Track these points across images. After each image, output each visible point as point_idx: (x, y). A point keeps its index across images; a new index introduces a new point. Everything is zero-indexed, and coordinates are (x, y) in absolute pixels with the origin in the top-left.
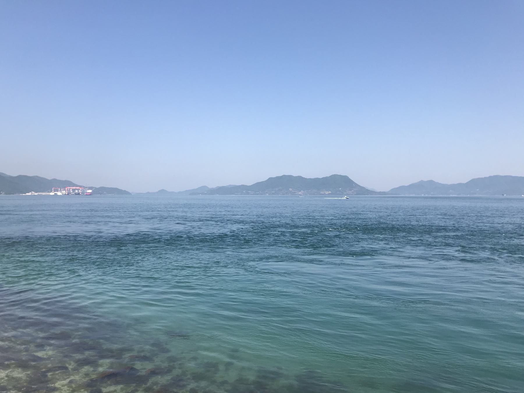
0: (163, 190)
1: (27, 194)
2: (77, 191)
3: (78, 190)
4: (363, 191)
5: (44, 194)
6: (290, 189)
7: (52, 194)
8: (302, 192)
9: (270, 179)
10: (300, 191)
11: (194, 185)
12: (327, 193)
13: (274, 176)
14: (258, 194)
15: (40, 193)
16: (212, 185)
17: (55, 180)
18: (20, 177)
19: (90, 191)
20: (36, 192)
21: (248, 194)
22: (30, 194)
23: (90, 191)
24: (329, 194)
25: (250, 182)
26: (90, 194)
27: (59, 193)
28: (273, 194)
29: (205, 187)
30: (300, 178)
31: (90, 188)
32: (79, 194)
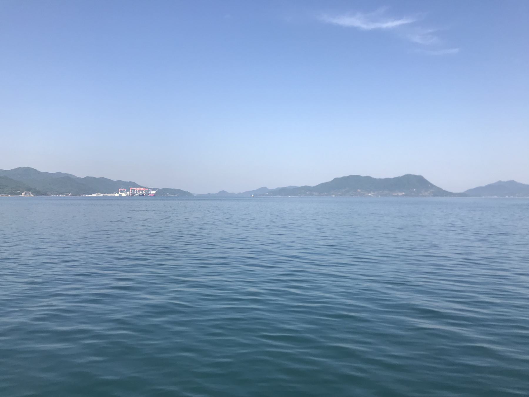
0: (223, 191)
1: (93, 195)
2: (141, 192)
3: (142, 191)
4: (439, 192)
5: (109, 195)
6: (359, 190)
7: (117, 195)
8: (372, 193)
9: (336, 180)
10: (369, 192)
11: (255, 187)
12: (400, 194)
13: (340, 176)
14: (323, 196)
15: (105, 195)
16: (273, 186)
17: (120, 181)
19: (154, 192)
21: (312, 195)
22: (95, 195)
23: (154, 192)
24: (403, 195)
25: (313, 183)
26: (154, 195)
27: (124, 195)
28: (341, 195)
29: (265, 188)
30: (368, 178)
31: (154, 189)
32: (143, 195)
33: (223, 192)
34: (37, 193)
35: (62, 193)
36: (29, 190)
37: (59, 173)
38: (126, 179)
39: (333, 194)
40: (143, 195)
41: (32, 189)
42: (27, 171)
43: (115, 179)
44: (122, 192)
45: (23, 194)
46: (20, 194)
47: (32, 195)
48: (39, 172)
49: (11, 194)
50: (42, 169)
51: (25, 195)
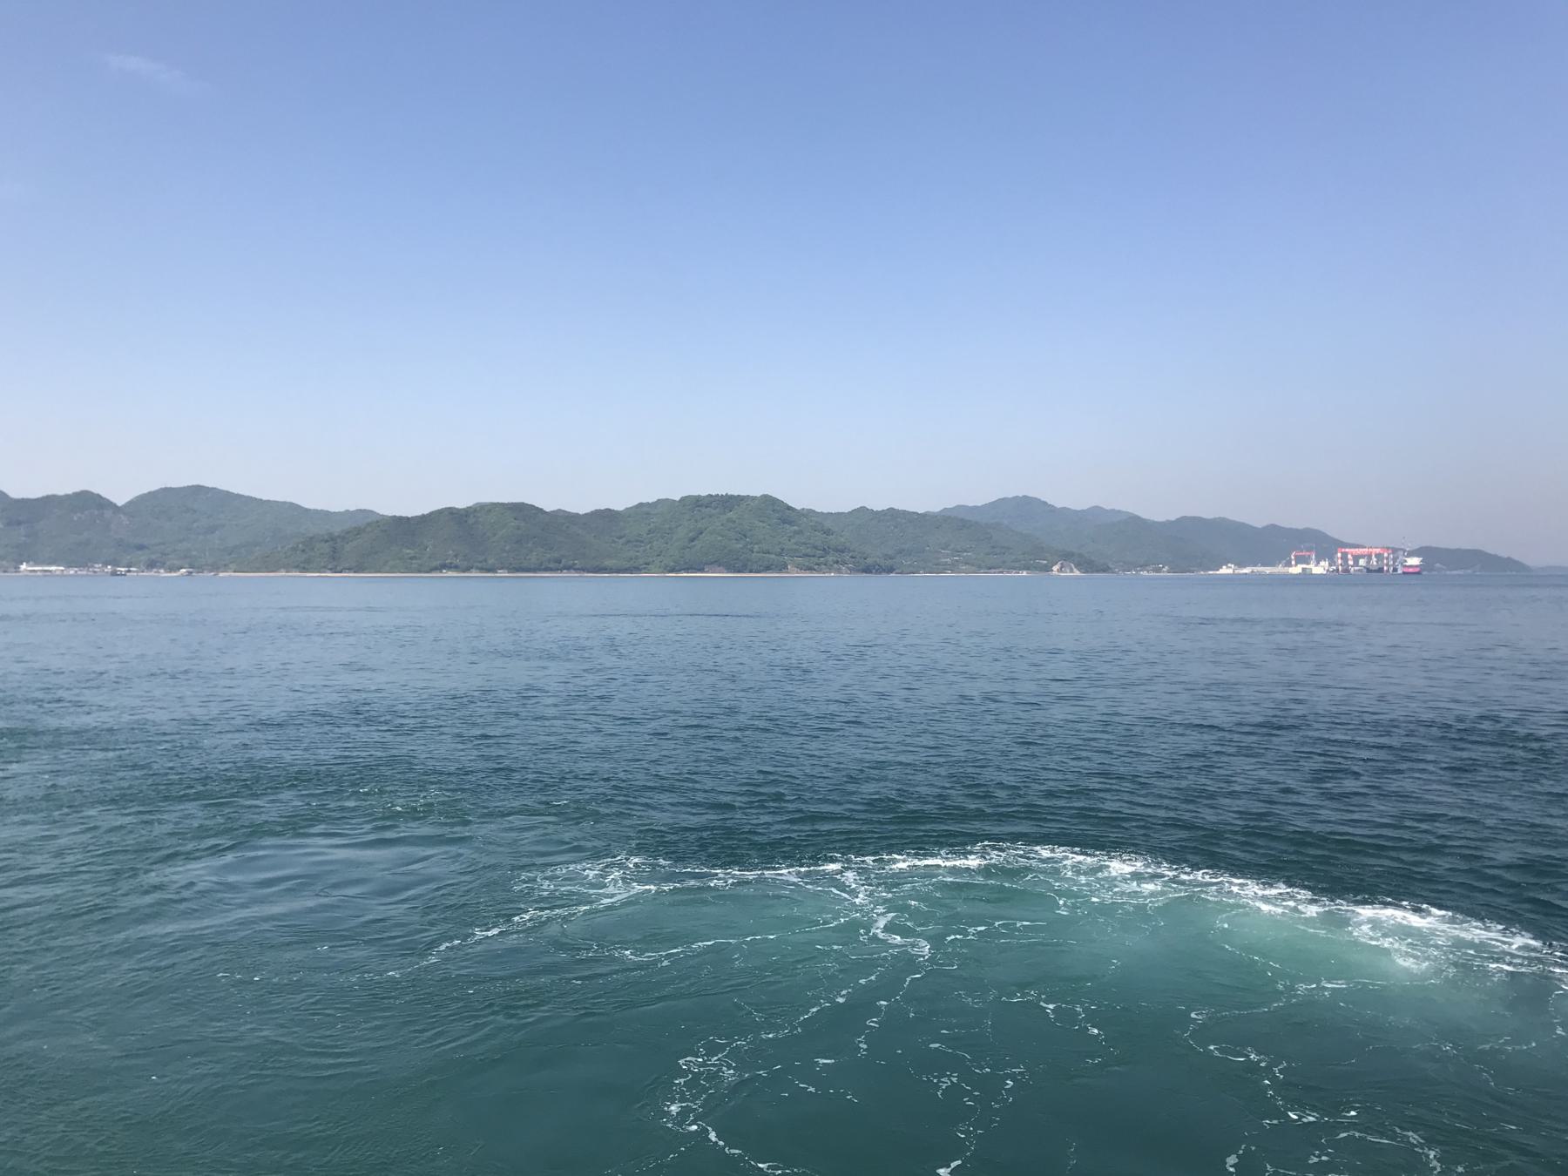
5: (1268, 570)
7: (1296, 570)
15: (1256, 569)
19: (1414, 561)
20: (1241, 565)
22: (1224, 570)
23: (1414, 561)
26: (1417, 572)
32: (1380, 570)
34: (1088, 565)
35: (1144, 566)
36: (1067, 557)
37: (1096, 510)
40: (1380, 570)
41: (1073, 554)
42: (1026, 506)
43: (1259, 521)
44: (1306, 560)
45: (1055, 568)
46: (1048, 569)
47: (1077, 573)
49: (1027, 568)
50: (1058, 501)
51: (1060, 570)
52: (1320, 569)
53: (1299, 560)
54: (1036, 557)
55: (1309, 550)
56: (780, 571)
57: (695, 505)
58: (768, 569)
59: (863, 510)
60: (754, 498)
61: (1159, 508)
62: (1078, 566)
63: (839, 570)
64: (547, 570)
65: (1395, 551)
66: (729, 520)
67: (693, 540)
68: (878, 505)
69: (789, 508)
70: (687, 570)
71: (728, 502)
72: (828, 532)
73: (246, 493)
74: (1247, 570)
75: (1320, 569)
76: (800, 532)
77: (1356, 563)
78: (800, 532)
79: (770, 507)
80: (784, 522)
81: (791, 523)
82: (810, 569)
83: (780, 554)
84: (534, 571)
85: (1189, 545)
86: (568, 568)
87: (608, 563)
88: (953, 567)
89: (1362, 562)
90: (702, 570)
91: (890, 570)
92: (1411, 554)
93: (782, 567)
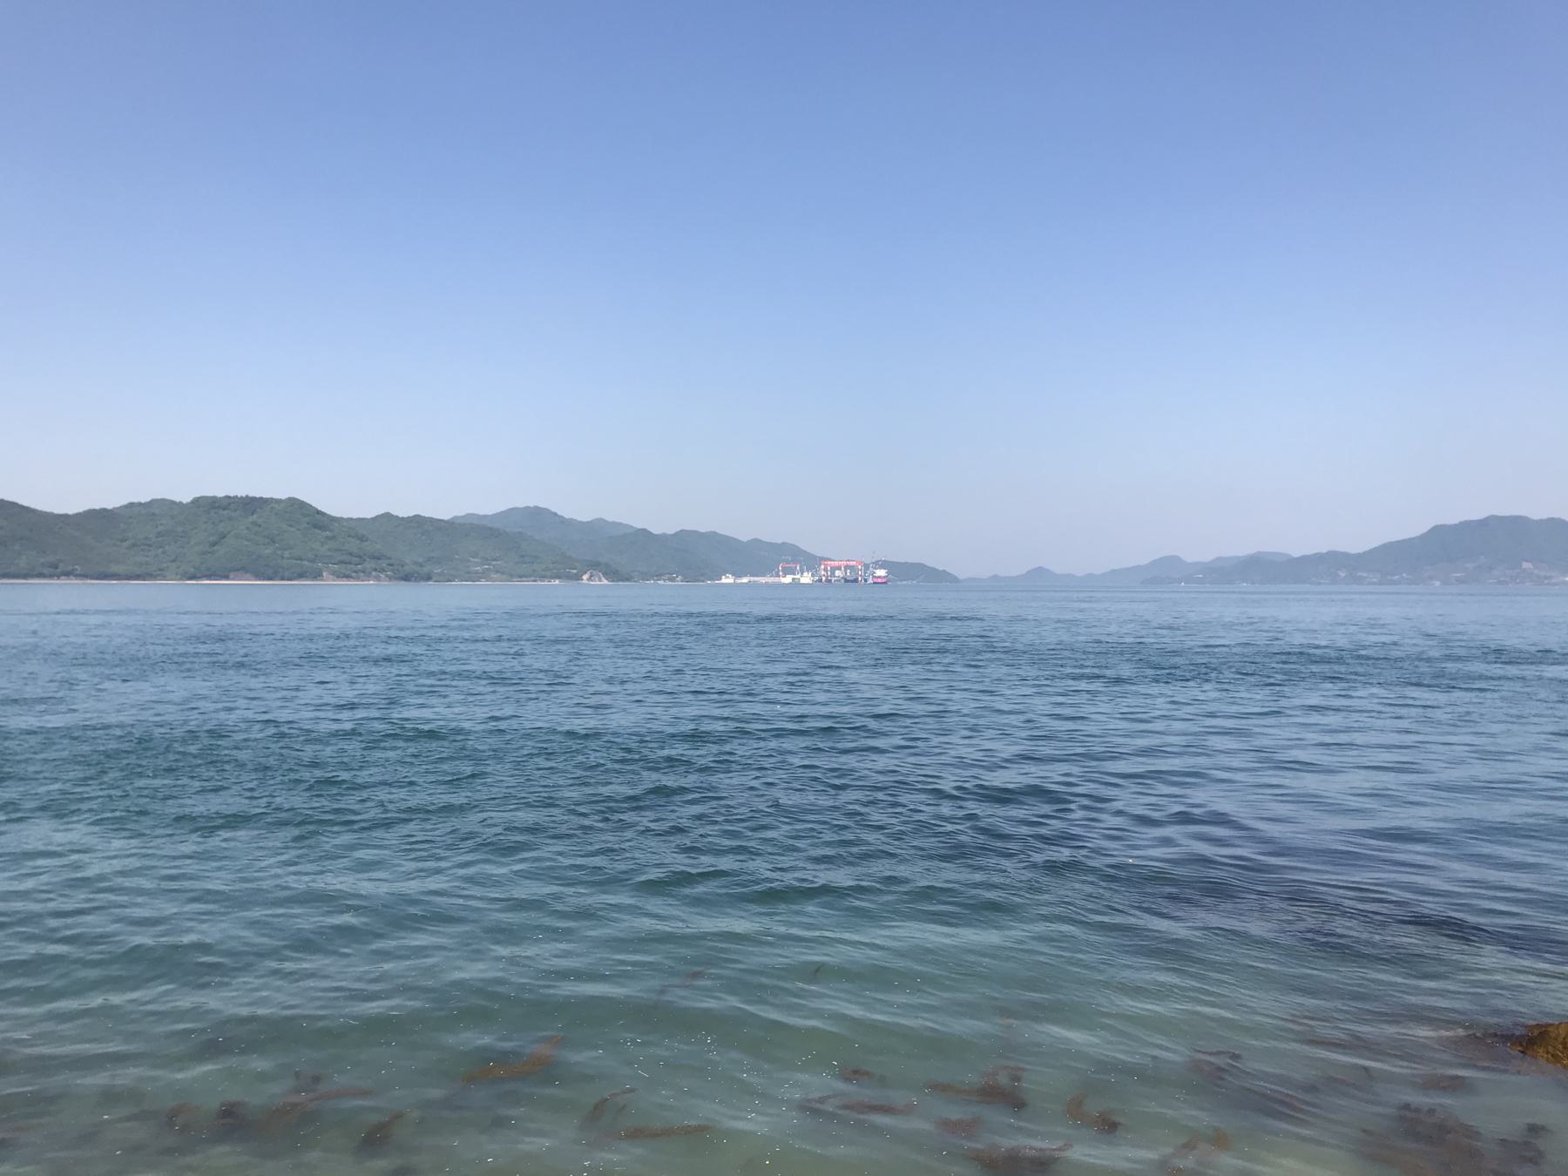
0: (1040, 568)
1: (724, 580)
5: (762, 580)
6: (1525, 565)
7: (788, 579)
9: (1438, 530)
11: (1141, 554)
13: (1452, 519)
17: (756, 540)
18: (682, 534)
19: (881, 573)
23: (881, 573)
27: (803, 580)
28: (1460, 581)
29: (1172, 561)
32: (856, 580)
33: (1040, 572)
34: (614, 574)
35: (659, 576)
38: (772, 534)
39: (1431, 578)
40: (856, 580)
43: (744, 537)
45: (585, 577)
46: (578, 577)
47: (605, 582)
48: (563, 522)
49: (559, 577)
52: (806, 579)
53: (786, 572)
54: (566, 567)
55: (796, 562)
56: (315, 578)
57: (1384, 546)
58: (301, 576)
59: (387, 516)
60: (278, 501)
61: (662, 523)
62: (606, 575)
63: (378, 578)
64: (41, 575)
65: (867, 567)
66: (254, 523)
67: (214, 544)
68: (403, 511)
69: (319, 512)
70: (209, 577)
71: (251, 505)
72: (362, 539)
73: (241, 493)
74: (745, 580)
75: (806, 579)
76: (333, 538)
77: (833, 574)
78: (333, 538)
79: (296, 510)
80: (315, 526)
81: (322, 528)
82: (348, 577)
83: (312, 561)
84: (25, 576)
85: (691, 555)
86: (67, 574)
87: (114, 569)
88: (484, 575)
89: (837, 573)
90: (227, 578)
91: (429, 578)
92: (882, 567)
93: (317, 575)
